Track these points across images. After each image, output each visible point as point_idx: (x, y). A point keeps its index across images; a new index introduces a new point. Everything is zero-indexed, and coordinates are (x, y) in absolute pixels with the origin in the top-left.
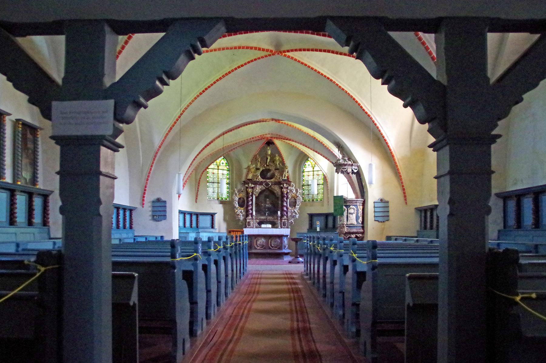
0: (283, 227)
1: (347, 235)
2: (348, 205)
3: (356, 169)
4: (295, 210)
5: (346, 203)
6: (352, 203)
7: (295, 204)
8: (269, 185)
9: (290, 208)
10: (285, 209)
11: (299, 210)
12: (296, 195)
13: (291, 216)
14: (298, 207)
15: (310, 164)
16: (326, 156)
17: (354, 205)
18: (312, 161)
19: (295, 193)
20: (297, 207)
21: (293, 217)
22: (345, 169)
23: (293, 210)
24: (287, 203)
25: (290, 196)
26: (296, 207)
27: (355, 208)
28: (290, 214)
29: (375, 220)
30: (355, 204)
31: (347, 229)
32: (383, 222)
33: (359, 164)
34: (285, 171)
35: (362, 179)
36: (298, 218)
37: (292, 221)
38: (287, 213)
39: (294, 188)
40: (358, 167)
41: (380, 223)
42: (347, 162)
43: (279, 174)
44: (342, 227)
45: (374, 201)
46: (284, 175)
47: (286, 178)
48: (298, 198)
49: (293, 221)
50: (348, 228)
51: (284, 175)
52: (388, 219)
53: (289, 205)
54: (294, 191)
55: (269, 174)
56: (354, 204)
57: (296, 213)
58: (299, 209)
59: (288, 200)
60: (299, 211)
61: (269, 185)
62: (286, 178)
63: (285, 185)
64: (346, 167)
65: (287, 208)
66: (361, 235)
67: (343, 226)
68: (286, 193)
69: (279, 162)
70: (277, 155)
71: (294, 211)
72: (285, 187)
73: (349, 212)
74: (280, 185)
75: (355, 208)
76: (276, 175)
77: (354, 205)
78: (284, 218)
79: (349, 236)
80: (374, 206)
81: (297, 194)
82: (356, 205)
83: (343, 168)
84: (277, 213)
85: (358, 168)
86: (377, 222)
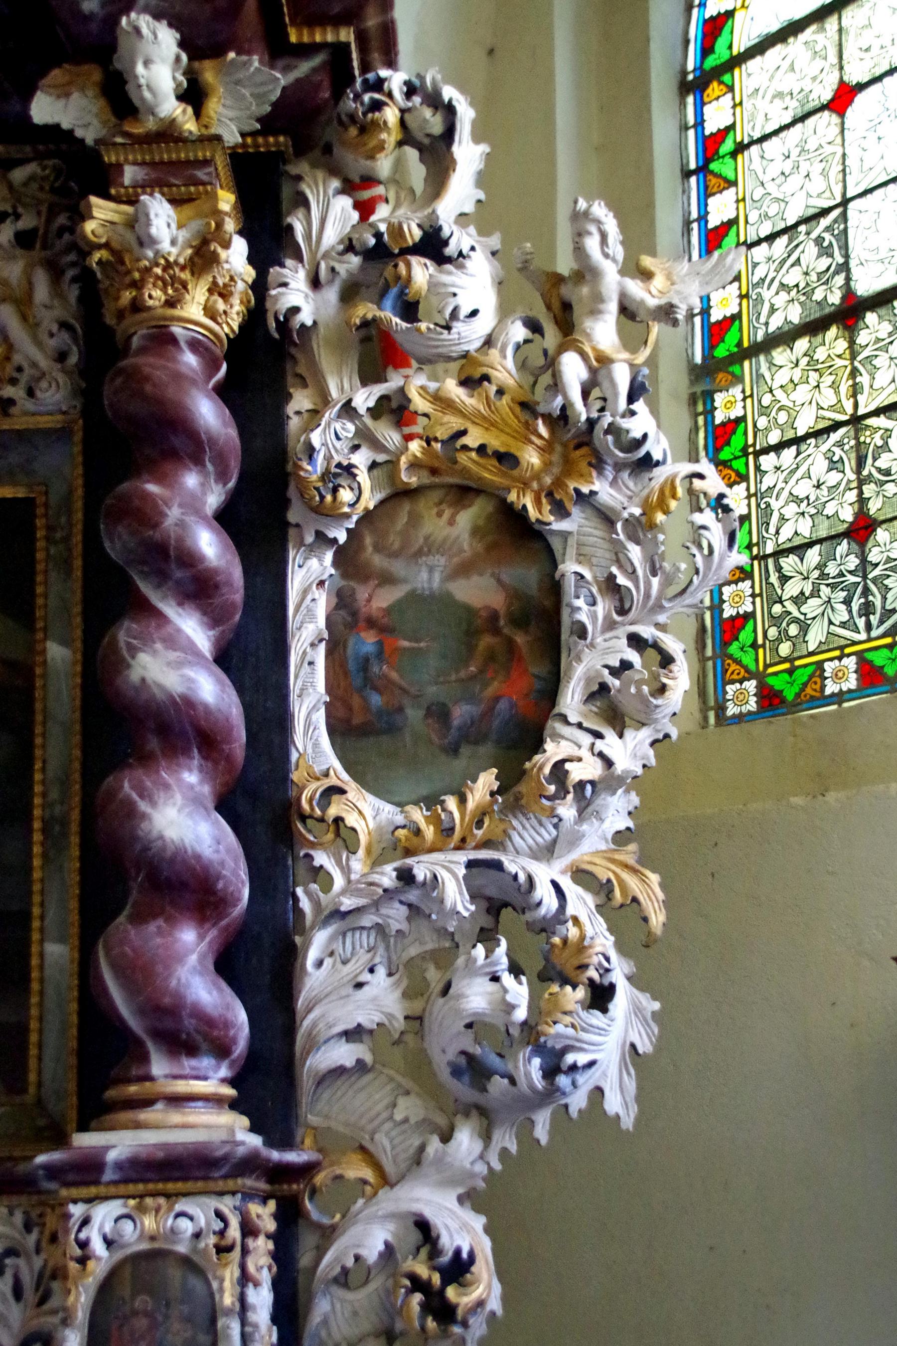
11: (646, 860)
26: (553, 751)
37: (423, 1226)
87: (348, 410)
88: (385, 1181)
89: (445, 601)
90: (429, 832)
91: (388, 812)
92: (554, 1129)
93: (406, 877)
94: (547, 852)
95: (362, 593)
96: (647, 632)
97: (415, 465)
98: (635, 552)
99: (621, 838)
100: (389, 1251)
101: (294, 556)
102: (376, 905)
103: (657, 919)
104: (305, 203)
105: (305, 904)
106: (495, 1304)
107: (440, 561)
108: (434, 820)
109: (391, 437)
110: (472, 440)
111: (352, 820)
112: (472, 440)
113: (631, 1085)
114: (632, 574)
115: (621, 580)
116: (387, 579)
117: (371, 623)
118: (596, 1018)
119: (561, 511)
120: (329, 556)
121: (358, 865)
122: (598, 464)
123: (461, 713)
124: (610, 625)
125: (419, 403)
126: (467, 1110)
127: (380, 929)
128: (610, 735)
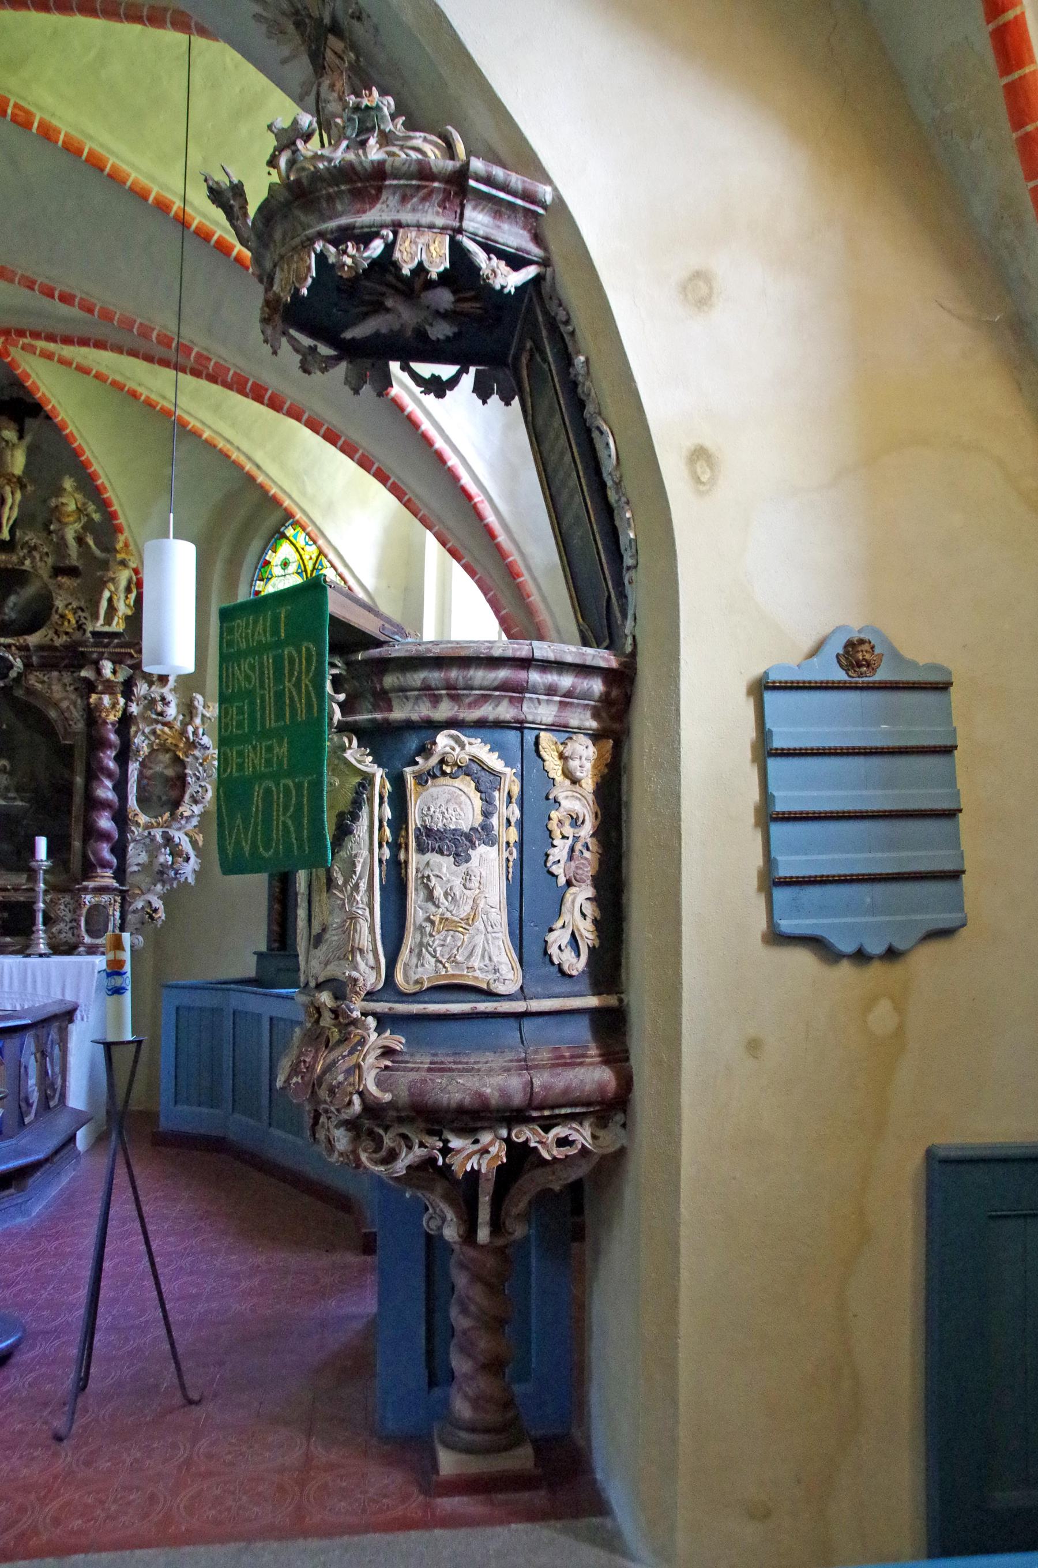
0: (87, 940)
1: (388, 1141)
2: (409, 726)
3: (516, 262)
4: (172, 832)
5: (383, 699)
6: (454, 692)
7: (174, 794)
8: (12, 666)
9: (143, 819)
10: (105, 822)
12: (183, 733)
13: (145, 868)
14: (197, 809)
15: (293, 557)
16: (332, 419)
17: (481, 725)
18: (301, 539)
19: (178, 725)
20: (185, 809)
21: (161, 874)
22: (365, 238)
23: (158, 834)
24: (121, 787)
25: (141, 742)
26: (181, 809)
27: (493, 761)
28: (143, 858)
29: (776, 938)
30: (505, 711)
31: (388, 1052)
32: (892, 954)
33: (546, 193)
34: (113, 580)
35: (586, 386)
36: (191, 880)
37: (150, 903)
38: (120, 850)
39: (174, 690)
40: (537, 239)
41: (845, 968)
42: (386, 139)
43: (75, 605)
44: (327, 1020)
45: (756, 670)
46: (104, 604)
47: (118, 625)
48: (197, 753)
49: (158, 903)
50: (397, 1041)
51: (104, 604)
52: (943, 919)
53: (140, 801)
54: (172, 711)
55: (12, 599)
56: (487, 711)
57: (176, 852)
58: (200, 827)
59: (134, 768)
60: (200, 838)
61: (12, 666)
62: (118, 625)
63: (107, 667)
64: (373, 215)
65: (121, 818)
66: (582, 1135)
67: (335, 1012)
68: (112, 718)
69: (78, 526)
70: (68, 484)
71: (168, 840)
72: (108, 681)
73: (414, 819)
74: (81, 667)
75: (493, 761)
76: (59, 603)
77: (481, 725)
78: (91, 884)
79: (418, 1152)
80: (763, 733)
81: (190, 729)
82: (519, 726)
83: (341, 237)
84: (32, 850)
85: (535, 251)
86: (803, 958)
87: (143, 733)
88: (143, 893)
89: (162, 773)
90: (155, 824)
91: (147, 819)
92: (178, 885)
93: (149, 833)
94: (179, 829)
95: (145, 771)
96: (203, 784)
97: (157, 745)
98: (201, 769)
99: (195, 827)
100: (143, 908)
101: (130, 763)
102: (143, 839)
103: (201, 843)
104: (136, 685)
105: (129, 837)
106: (163, 918)
107: (162, 765)
108: (156, 822)
109: (152, 738)
110: (169, 741)
111: (139, 821)
112: (169, 741)
113: (194, 876)
114: (199, 772)
115: (198, 774)
116: (150, 768)
117: (146, 778)
118: (185, 864)
119: (187, 757)
120: (138, 763)
121: (140, 830)
122: (196, 747)
123: (164, 798)
124: (195, 782)
125: (158, 732)
126: (159, 881)
127: (144, 843)
128: (194, 806)
